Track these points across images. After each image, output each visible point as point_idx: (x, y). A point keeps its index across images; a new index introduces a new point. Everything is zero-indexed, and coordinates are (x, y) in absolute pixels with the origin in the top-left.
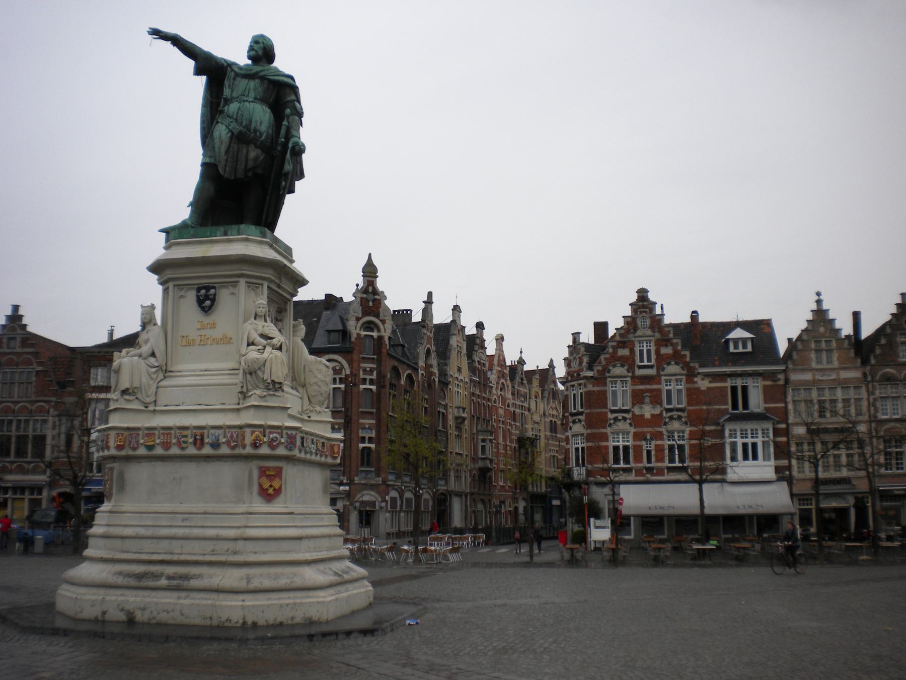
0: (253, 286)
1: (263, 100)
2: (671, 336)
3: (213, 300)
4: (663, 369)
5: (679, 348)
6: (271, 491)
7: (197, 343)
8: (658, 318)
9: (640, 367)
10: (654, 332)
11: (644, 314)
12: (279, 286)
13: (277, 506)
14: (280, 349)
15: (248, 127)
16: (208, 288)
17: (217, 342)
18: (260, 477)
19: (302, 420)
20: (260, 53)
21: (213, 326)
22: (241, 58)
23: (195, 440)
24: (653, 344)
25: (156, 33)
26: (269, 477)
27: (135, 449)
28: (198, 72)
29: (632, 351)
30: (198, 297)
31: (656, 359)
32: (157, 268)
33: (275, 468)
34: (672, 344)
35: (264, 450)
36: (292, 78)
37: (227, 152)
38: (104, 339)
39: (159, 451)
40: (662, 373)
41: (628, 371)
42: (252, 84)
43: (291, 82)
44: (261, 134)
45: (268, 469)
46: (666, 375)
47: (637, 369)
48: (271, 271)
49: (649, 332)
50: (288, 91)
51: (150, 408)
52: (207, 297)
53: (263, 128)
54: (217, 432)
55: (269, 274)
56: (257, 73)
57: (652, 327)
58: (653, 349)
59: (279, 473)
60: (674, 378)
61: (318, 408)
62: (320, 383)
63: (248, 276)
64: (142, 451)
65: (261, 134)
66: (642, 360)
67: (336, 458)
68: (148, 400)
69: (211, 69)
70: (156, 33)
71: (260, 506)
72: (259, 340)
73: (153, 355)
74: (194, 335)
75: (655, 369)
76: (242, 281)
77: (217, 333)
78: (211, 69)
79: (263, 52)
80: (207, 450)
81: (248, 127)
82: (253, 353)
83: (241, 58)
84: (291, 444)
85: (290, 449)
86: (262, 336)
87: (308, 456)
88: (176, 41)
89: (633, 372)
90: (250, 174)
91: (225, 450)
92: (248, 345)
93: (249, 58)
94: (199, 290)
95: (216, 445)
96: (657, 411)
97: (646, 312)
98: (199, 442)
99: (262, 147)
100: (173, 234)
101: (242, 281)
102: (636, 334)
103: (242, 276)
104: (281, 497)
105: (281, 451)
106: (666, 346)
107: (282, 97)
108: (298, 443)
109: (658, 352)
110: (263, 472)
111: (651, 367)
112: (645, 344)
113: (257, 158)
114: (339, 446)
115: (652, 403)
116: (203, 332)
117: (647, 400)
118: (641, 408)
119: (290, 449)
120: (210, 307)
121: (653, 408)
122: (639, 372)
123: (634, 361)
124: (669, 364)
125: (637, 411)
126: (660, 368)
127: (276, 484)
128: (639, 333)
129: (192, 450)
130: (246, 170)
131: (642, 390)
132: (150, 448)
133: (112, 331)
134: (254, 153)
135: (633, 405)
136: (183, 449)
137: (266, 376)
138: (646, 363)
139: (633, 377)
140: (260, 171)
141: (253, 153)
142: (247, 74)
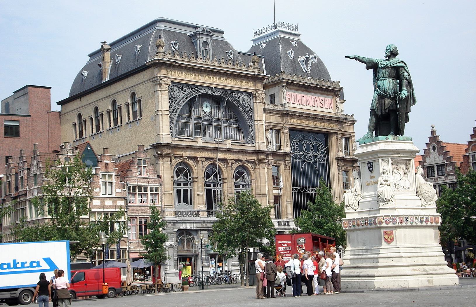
0: (385, 160)
3: (372, 168)
6: (389, 240)
13: (392, 245)
16: (370, 163)
20: (389, 54)
21: (374, 177)
26: (387, 234)
28: (368, 68)
36: (402, 62)
37: (377, 103)
39: (357, 227)
42: (384, 70)
43: (402, 64)
44: (389, 93)
59: (392, 233)
61: (429, 203)
63: (381, 157)
65: (389, 93)
68: (356, 208)
69: (373, 66)
70: (347, 57)
72: (384, 183)
78: (373, 66)
80: (369, 226)
85: (394, 224)
86: (386, 181)
87: (414, 224)
88: (356, 58)
90: (387, 111)
91: (373, 226)
98: (366, 223)
101: (380, 160)
103: (379, 157)
107: (398, 73)
113: (389, 103)
119: (394, 224)
127: (391, 237)
129: (365, 227)
134: (387, 101)
141: (387, 101)
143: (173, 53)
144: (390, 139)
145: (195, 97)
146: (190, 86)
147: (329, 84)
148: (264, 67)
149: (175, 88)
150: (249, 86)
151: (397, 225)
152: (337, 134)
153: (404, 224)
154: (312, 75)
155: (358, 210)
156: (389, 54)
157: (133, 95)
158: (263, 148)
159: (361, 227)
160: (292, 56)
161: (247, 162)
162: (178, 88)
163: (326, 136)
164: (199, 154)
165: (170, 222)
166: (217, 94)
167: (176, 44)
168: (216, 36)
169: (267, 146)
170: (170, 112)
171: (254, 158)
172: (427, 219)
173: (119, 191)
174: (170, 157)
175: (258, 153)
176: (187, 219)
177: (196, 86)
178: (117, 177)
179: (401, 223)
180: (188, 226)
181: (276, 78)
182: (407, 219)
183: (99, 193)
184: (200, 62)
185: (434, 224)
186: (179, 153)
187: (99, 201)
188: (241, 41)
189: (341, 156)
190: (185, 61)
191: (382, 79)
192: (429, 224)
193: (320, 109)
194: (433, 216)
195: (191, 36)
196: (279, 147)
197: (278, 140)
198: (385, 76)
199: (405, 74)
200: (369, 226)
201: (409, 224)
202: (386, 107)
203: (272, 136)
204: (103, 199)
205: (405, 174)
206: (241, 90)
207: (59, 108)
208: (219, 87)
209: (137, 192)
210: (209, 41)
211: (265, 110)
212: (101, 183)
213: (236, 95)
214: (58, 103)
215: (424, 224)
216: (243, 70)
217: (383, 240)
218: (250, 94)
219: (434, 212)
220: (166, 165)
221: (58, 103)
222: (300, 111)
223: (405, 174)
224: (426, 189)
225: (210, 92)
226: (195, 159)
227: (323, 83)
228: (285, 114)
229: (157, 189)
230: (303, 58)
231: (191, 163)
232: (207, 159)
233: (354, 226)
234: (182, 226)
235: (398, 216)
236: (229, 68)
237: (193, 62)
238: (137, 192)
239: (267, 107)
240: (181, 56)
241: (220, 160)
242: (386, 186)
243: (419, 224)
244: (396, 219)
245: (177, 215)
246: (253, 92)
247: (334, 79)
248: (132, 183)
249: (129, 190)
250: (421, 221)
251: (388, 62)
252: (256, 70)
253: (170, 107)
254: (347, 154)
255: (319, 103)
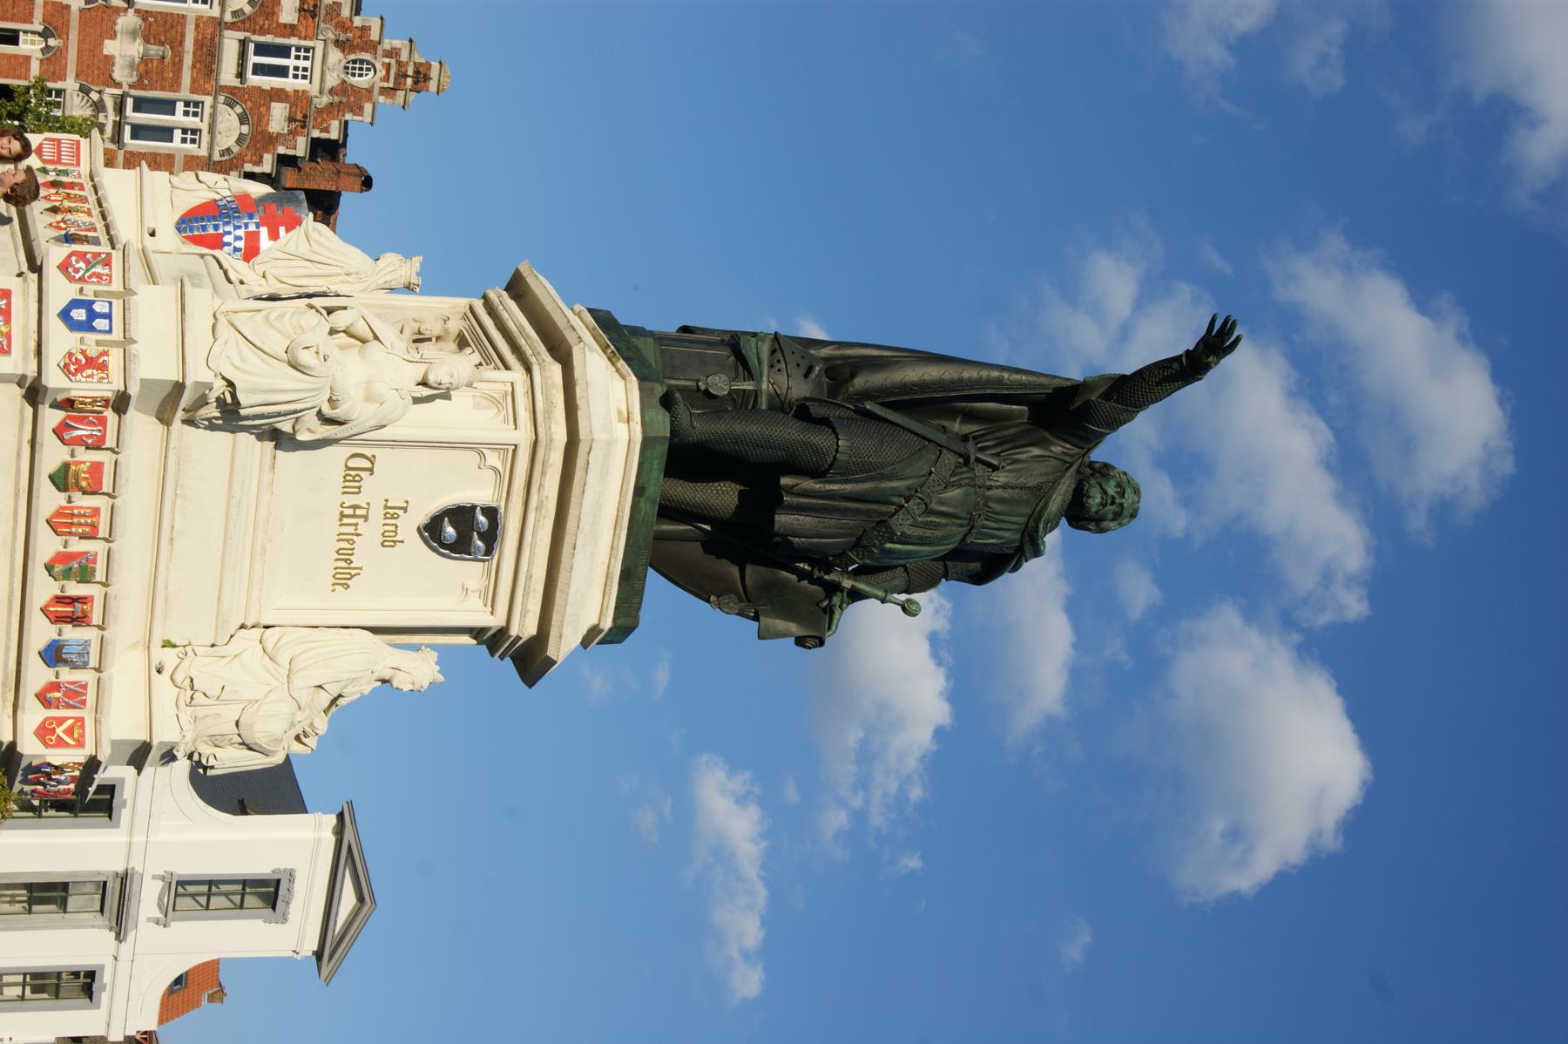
2: (316, 134)
4: (230, 104)
5: (282, 150)
7: (351, 500)
8: (368, 107)
9: (243, 44)
10: (331, 91)
11: (382, 73)
16: (491, 537)
17: (345, 556)
23: (73, 600)
24: (301, 84)
29: (291, 30)
30: (474, 507)
31: (260, 90)
34: (292, 133)
40: (221, 99)
41: (235, 13)
46: (214, 107)
47: (241, 35)
49: (332, 80)
57: (344, 88)
58: (288, 83)
60: (204, 127)
66: (262, 49)
74: (373, 491)
75: (236, 82)
77: (367, 550)
89: (232, 26)
94: (491, 513)
95: (54, 655)
96: (119, 74)
97: (386, 79)
102: (331, 47)
106: (291, 119)
109: (278, 95)
111: (241, 75)
112: (302, 63)
115: (145, 60)
116: (377, 513)
117: (155, 50)
118: (133, 34)
121: (131, 65)
122: (230, 44)
123: (263, 32)
124: (243, 119)
125: (128, 21)
126: (233, 96)
128: (335, 55)
131: (181, 43)
135: (144, 14)
138: (254, 59)
139: (219, 24)
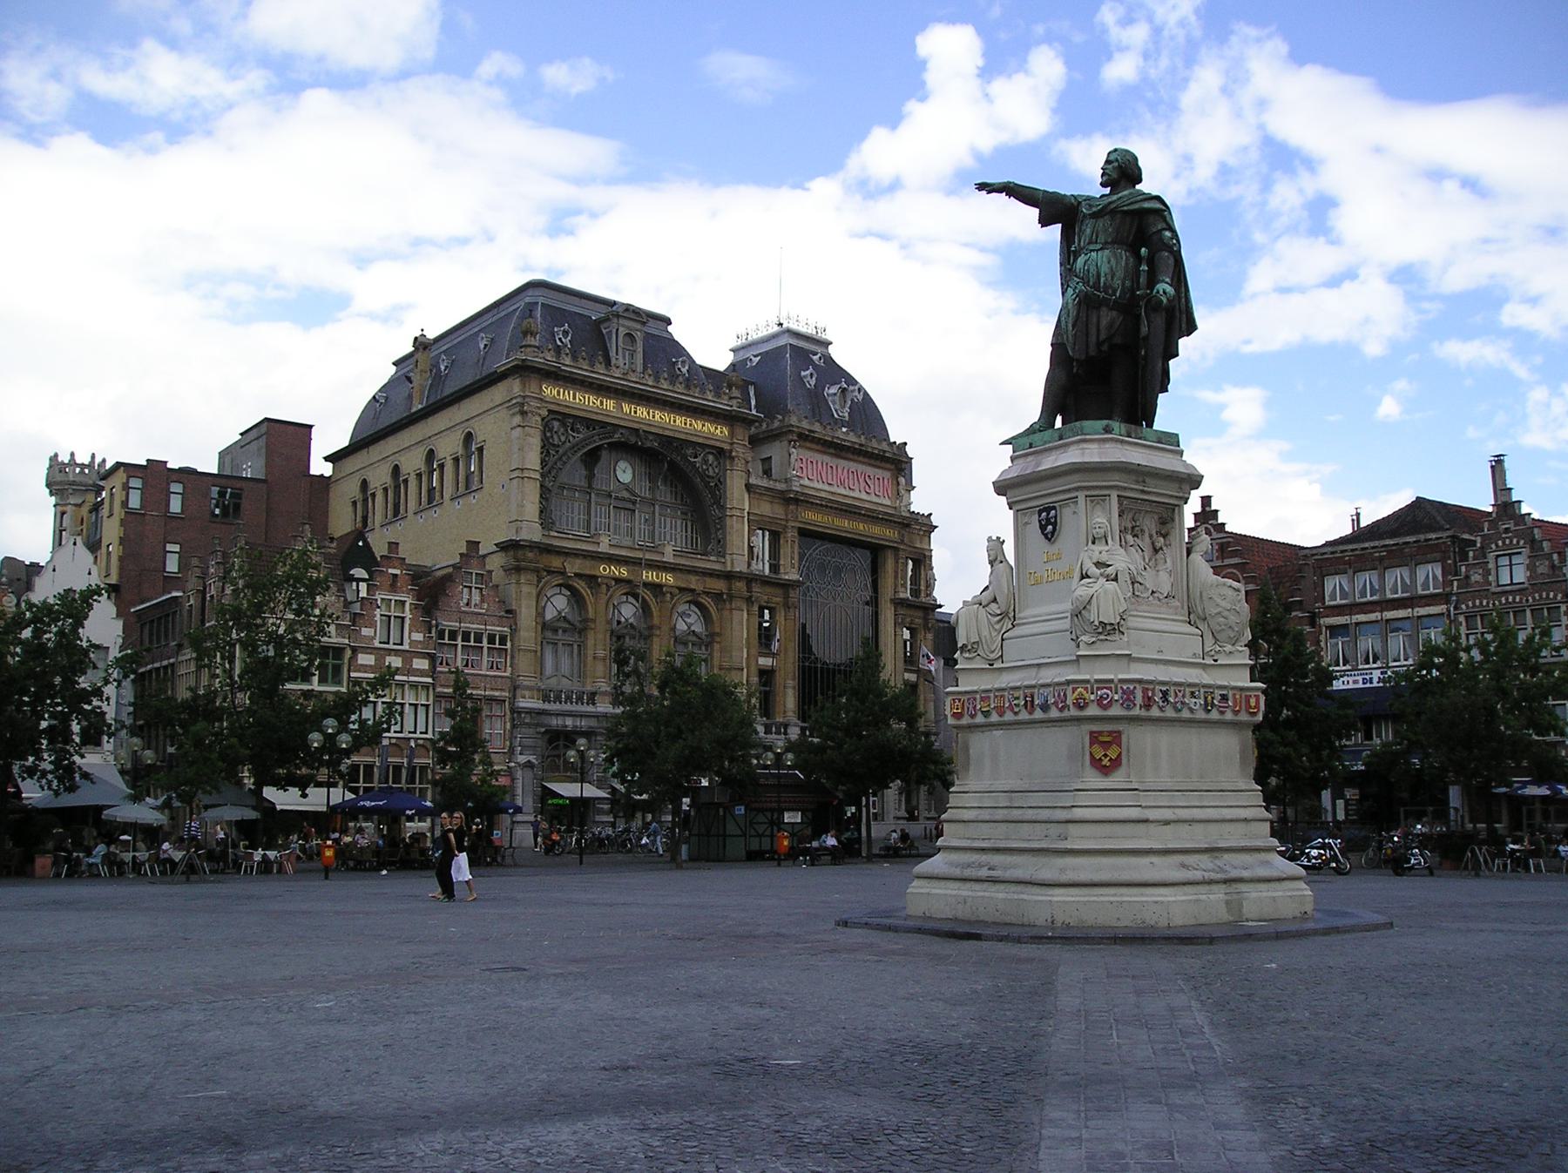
0: (1097, 499)
1: (1117, 242)
3: (1055, 525)
6: (1106, 762)
12: (1143, 492)
13: (1117, 779)
14: (1116, 579)
15: (1096, 286)
16: (1048, 510)
18: (1091, 744)
19: (1204, 667)
20: (1115, 175)
22: (1093, 187)
25: (982, 187)
27: (973, 716)
28: (1045, 221)
32: (1001, 488)
33: (1110, 733)
35: (1093, 711)
36: (1158, 198)
38: (1347, 530)
39: (994, 718)
42: (1100, 223)
44: (1114, 292)
45: (1100, 733)
48: (1117, 476)
50: (1151, 219)
51: (991, 668)
52: (1048, 522)
53: (1117, 282)
54: (1045, 691)
55: (1116, 480)
56: (1105, 207)
59: (1116, 738)
61: (1229, 648)
62: (1226, 613)
64: (980, 719)
67: (1254, 714)
68: (992, 656)
71: (1094, 779)
73: (995, 600)
76: (1081, 495)
79: (1123, 171)
80: (1038, 714)
81: (1096, 286)
82: (1082, 590)
83: (1093, 187)
84: (1148, 703)
85: (1128, 708)
86: (1098, 564)
87: (1186, 714)
88: (1012, 190)
90: (1105, 347)
91: (1054, 713)
92: (1083, 578)
93: (1103, 185)
95: (1045, 707)
99: (1115, 306)
100: (1022, 444)
104: (1122, 771)
105: (1116, 711)
108: (1139, 700)
110: (1094, 738)
113: (1111, 325)
114: (1257, 697)
120: (1053, 533)
129: (1024, 716)
130: (1099, 344)
132: (986, 714)
133: (1358, 515)
134: (1107, 317)
136: (1016, 714)
137: (1093, 617)
140: (1118, 340)
141: (1107, 317)
142: (1104, 211)
143: (558, 350)
144: (1117, 430)
145: (599, 448)
146: (589, 423)
147: (884, 446)
148: (753, 403)
149: (556, 424)
150: (717, 432)
151: (1136, 711)
152: (896, 549)
153: (1155, 712)
154: (850, 425)
155: (997, 665)
156: (1115, 175)
157: (469, 437)
158: (740, 566)
159: (1009, 716)
160: (813, 382)
161: (707, 594)
162: (564, 425)
163: (876, 551)
164: (604, 570)
165: (530, 712)
166: (648, 444)
167: (566, 333)
168: (652, 328)
169: (749, 565)
170: (542, 475)
171: (719, 585)
172: (1224, 698)
173: (418, 637)
174: (537, 571)
175: (729, 576)
176: (568, 707)
177: (604, 425)
178: (415, 607)
179: (1147, 706)
180: (569, 722)
181: (776, 424)
182: (1165, 694)
183: (373, 638)
184: (614, 376)
185: (1244, 717)
186: (556, 562)
187: (373, 657)
188: (710, 347)
189: (902, 595)
190: (582, 370)
191: (1091, 247)
192: (1229, 716)
193: (864, 496)
194: (1242, 689)
195: (599, 322)
196: (775, 568)
197: (775, 554)
198: (1102, 239)
199: (1168, 234)
200: (1038, 714)
201: (1170, 713)
202: (1103, 337)
203: (762, 542)
204: (381, 653)
205: (1156, 551)
206: (701, 441)
207: (326, 469)
208: (653, 430)
209: (459, 642)
210: (638, 336)
211: (748, 487)
212: (378, 618)
213: (690, 451)
214: (327, 459)
215: (1214, 715)
216: (709, 400)
217: (1088, 762)
218: (720, 453)
219: (1243, 680)
220: (525, 589)
221: (327, 459)
222: (823, 495)
223: (1156, 551)
224: (1223, 603)
225: (633, 440)
226: (592, 580)
227: (874, 444)
228: (793, 500)
229: (503, 640)
230: (833, 390)
231: (580, 585)
232: (618, 580)
233: (986, 714)
234: (555, 722)
235: (1140, 681)
236: (678, 392)
237: (600, 373)
238: (459, 642)
239: (752, 481)
240: (575, 358)
241: (646, 585)
242: (1102, 580)
243: (1201, 715)
244: (1133, 692)
245: (546, 699)
246: (726, 447)
247: (895, 436)
248: (449, 624)
249: (441, 635)
250: (1206, 704)
251: (1115, 197)
252: (734, 402)
253: (543, 463)
254: (916, 592)
255: (863, 484)
